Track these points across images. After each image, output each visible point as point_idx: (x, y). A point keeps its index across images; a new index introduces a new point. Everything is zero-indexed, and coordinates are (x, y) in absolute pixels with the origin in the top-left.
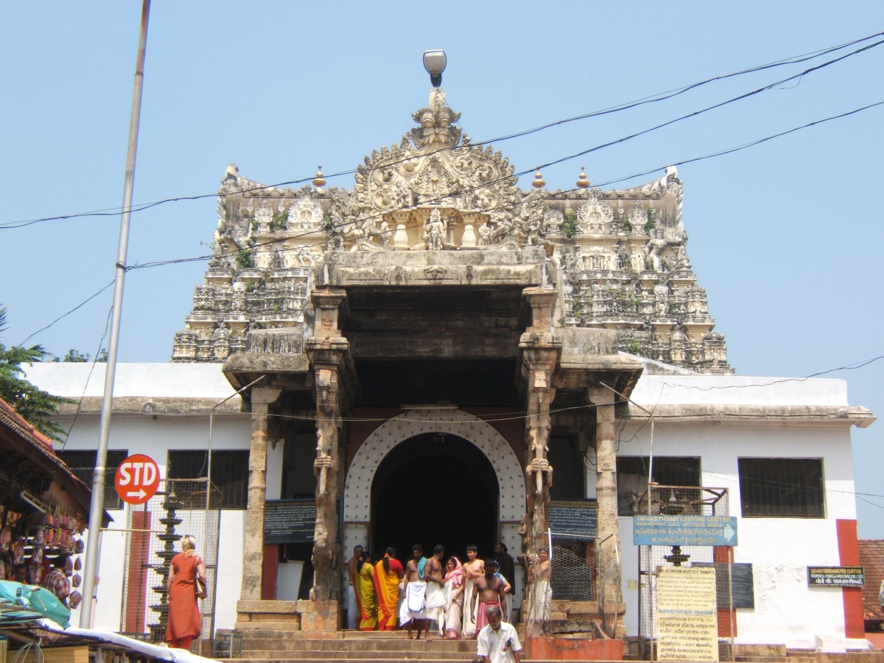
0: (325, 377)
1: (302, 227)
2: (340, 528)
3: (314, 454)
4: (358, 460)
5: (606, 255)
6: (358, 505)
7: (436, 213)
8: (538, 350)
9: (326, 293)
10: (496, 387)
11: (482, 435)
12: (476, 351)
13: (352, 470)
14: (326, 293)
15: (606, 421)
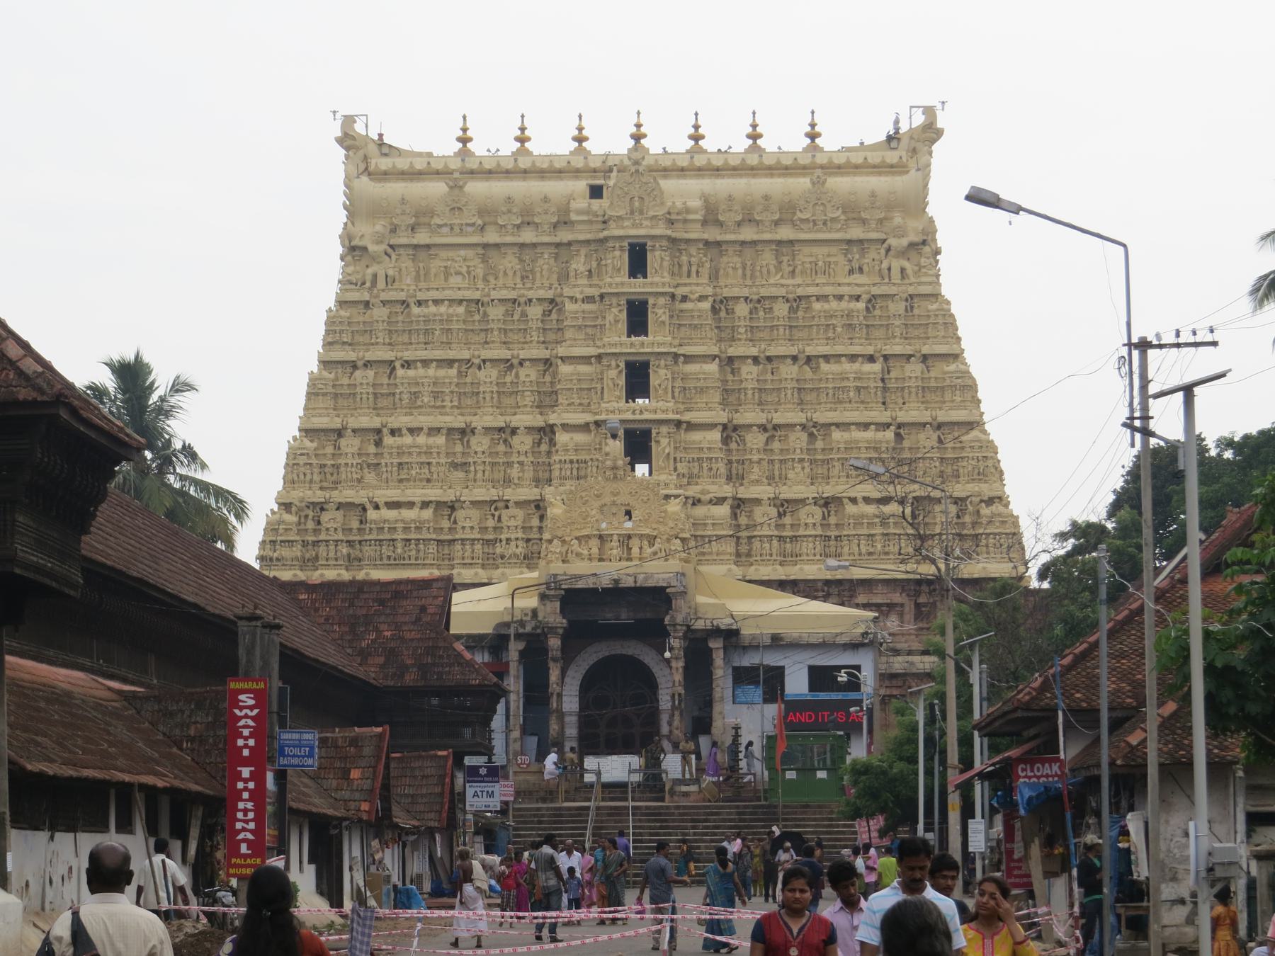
0: (554, 642)
1: (452, 229)
2: (561, 715)
3: (547, 686)
4: (570, 673)
5: (832, 259)
6: (571, 703)
7: (615, 538)
8: (674, 625)
9: (552, 593)
10: (655, 633)
11: (648, 657)
12: (641, 615)
13: (567, 680)
14: (552, 593)
15: (718, 659)
